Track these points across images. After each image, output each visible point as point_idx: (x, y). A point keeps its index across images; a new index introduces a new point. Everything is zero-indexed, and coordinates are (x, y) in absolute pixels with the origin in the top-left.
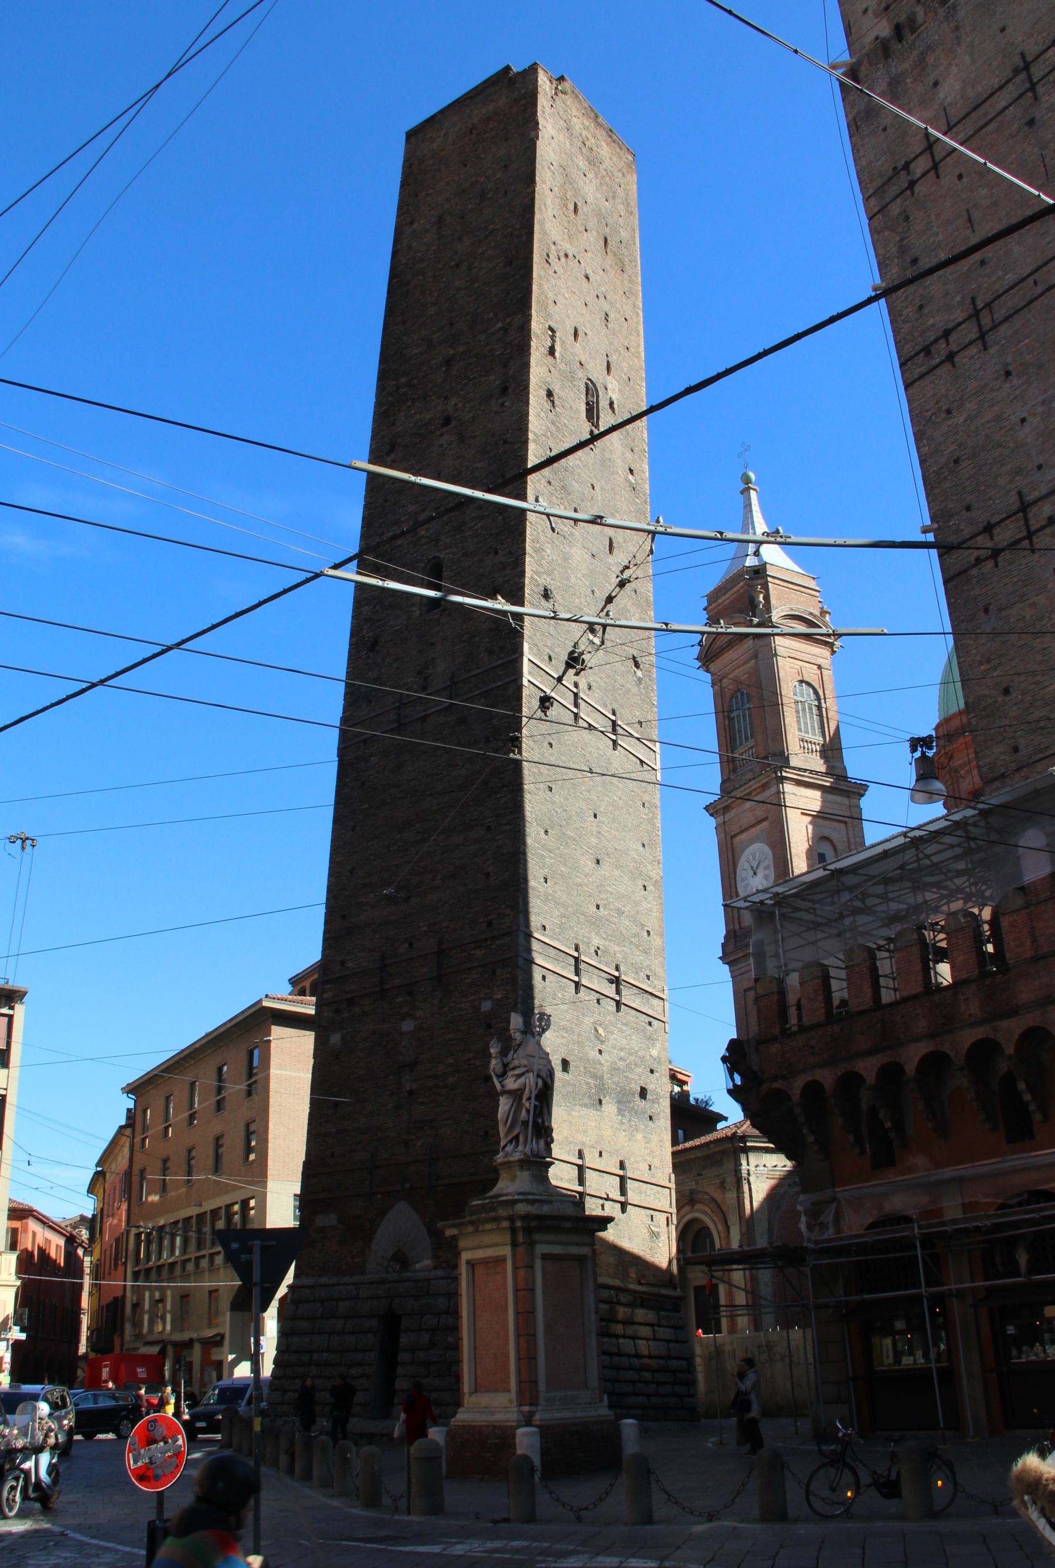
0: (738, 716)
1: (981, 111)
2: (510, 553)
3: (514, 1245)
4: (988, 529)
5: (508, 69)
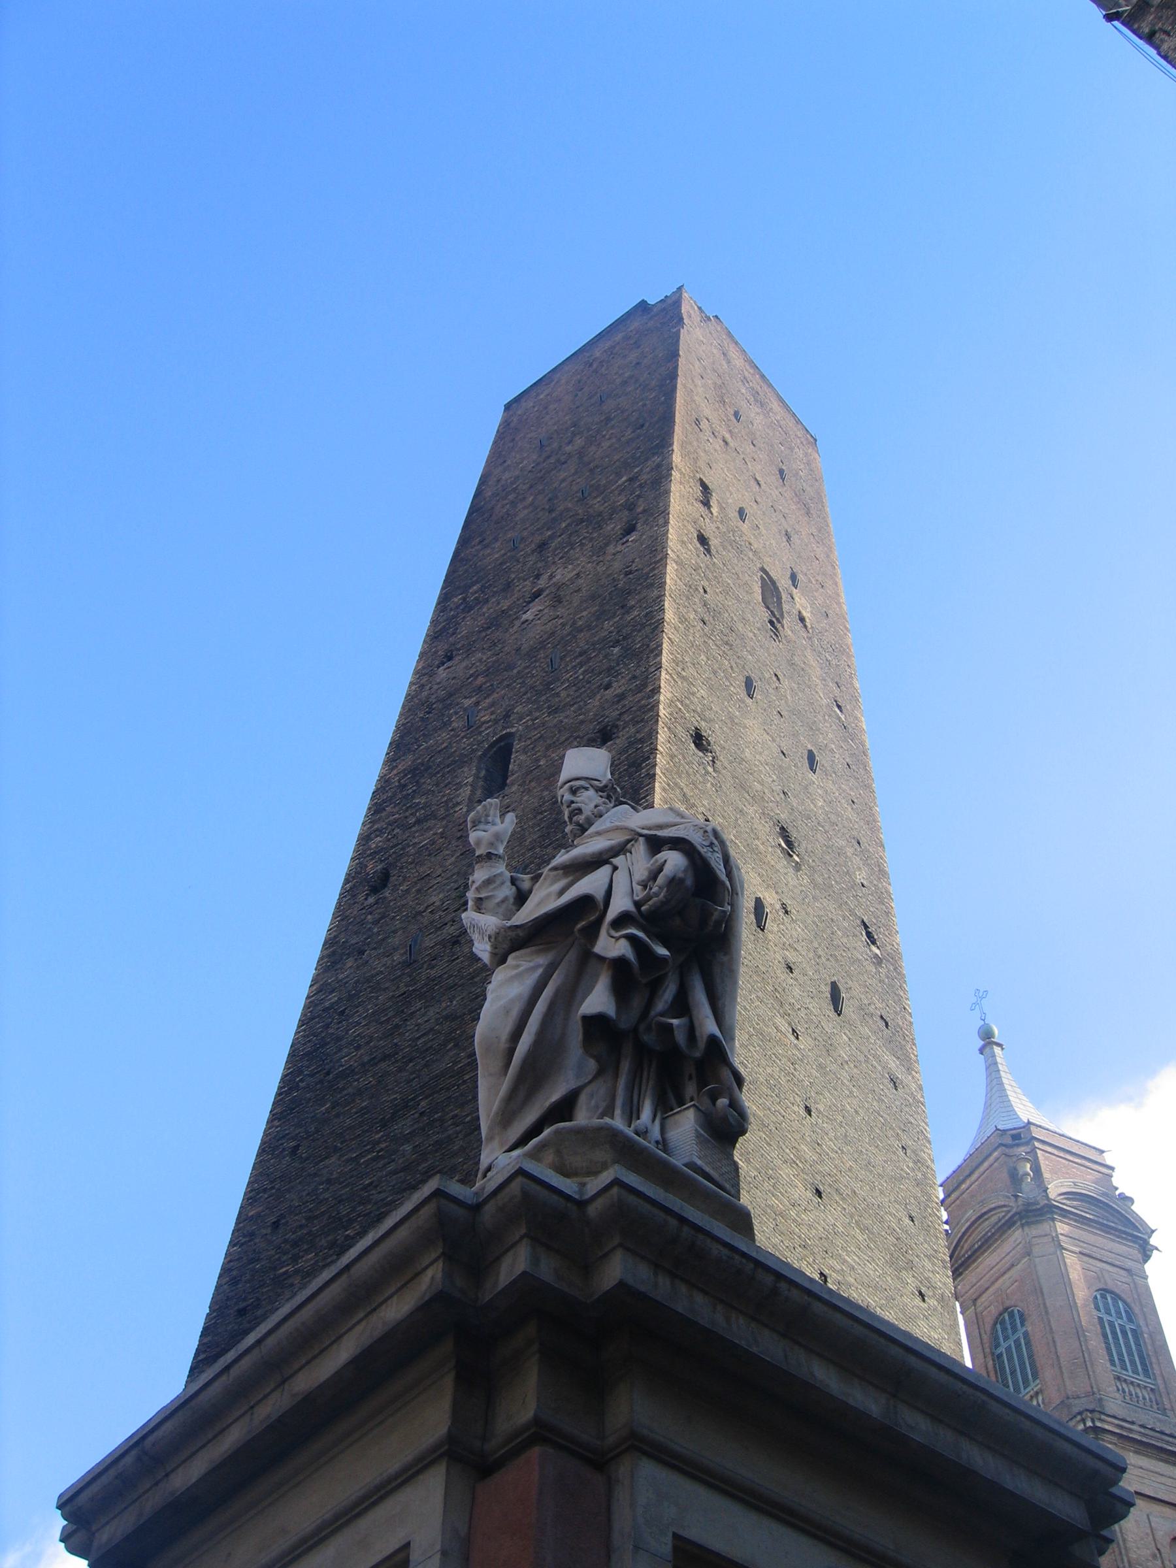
0: (1008, 1349)
2: (634, 677)
3: (471, 1459)
5: (643, 302)
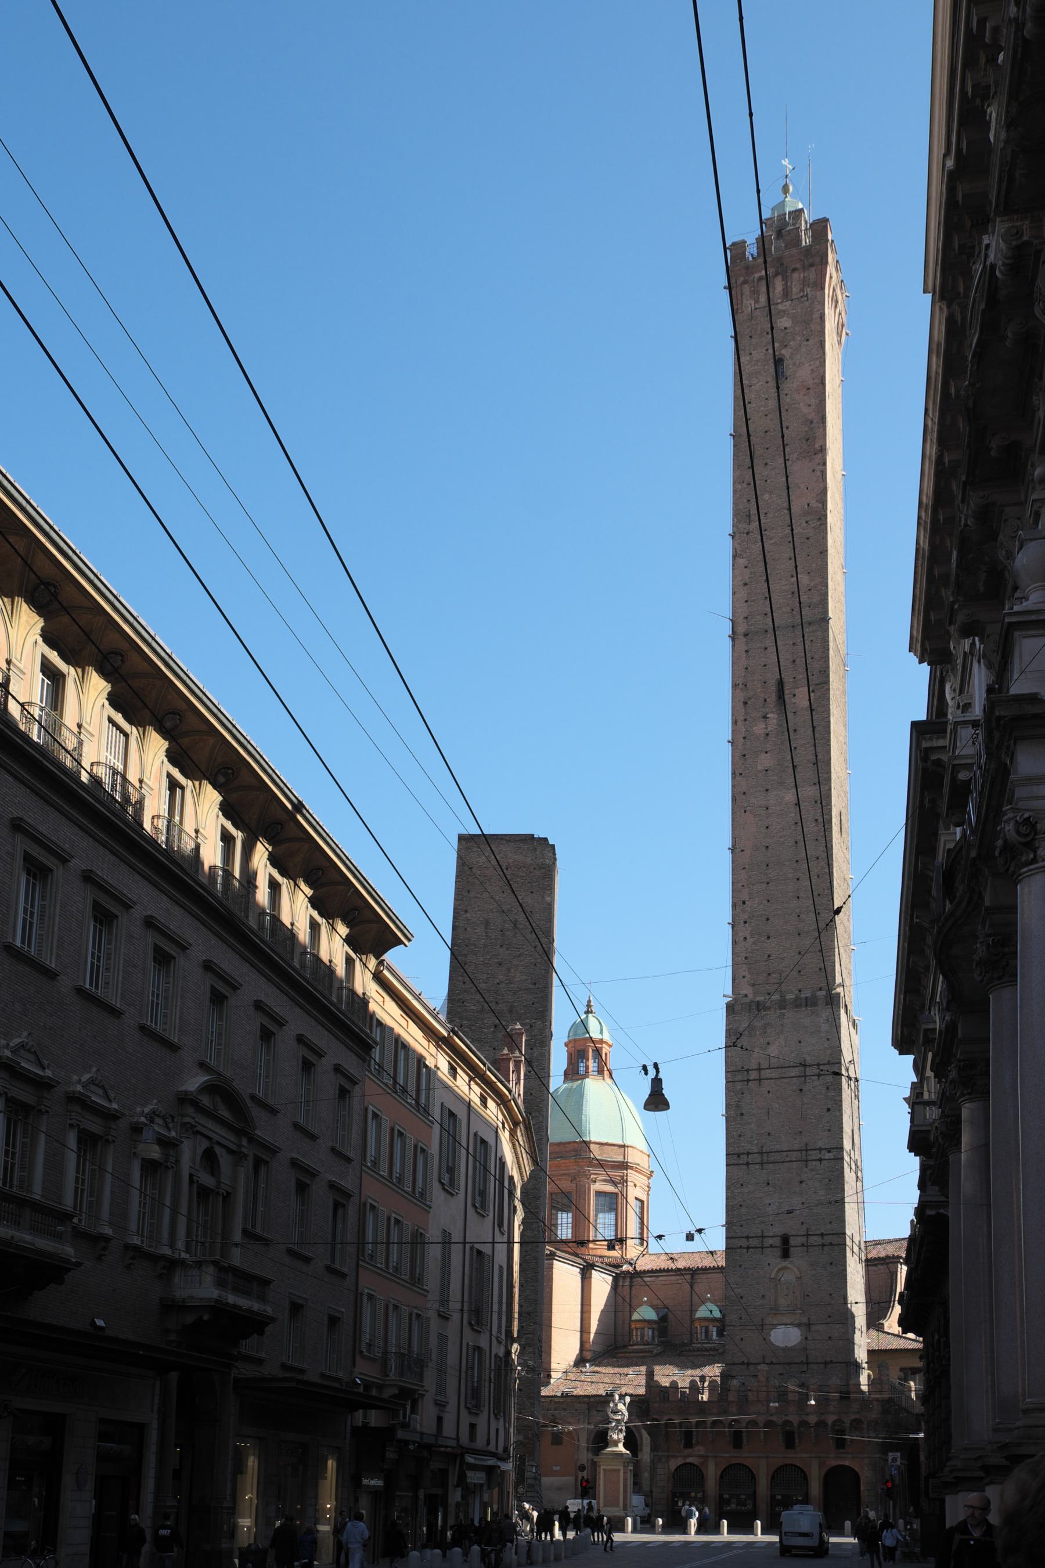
1: (784, 1070)
4: (748, 1237)
